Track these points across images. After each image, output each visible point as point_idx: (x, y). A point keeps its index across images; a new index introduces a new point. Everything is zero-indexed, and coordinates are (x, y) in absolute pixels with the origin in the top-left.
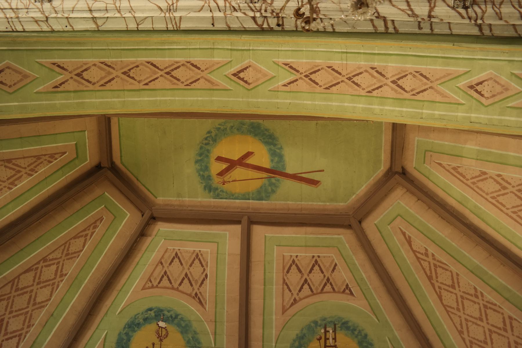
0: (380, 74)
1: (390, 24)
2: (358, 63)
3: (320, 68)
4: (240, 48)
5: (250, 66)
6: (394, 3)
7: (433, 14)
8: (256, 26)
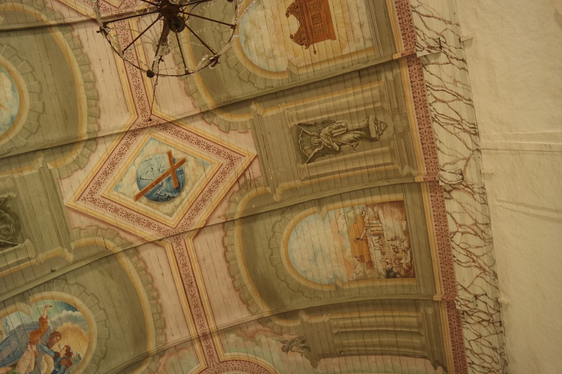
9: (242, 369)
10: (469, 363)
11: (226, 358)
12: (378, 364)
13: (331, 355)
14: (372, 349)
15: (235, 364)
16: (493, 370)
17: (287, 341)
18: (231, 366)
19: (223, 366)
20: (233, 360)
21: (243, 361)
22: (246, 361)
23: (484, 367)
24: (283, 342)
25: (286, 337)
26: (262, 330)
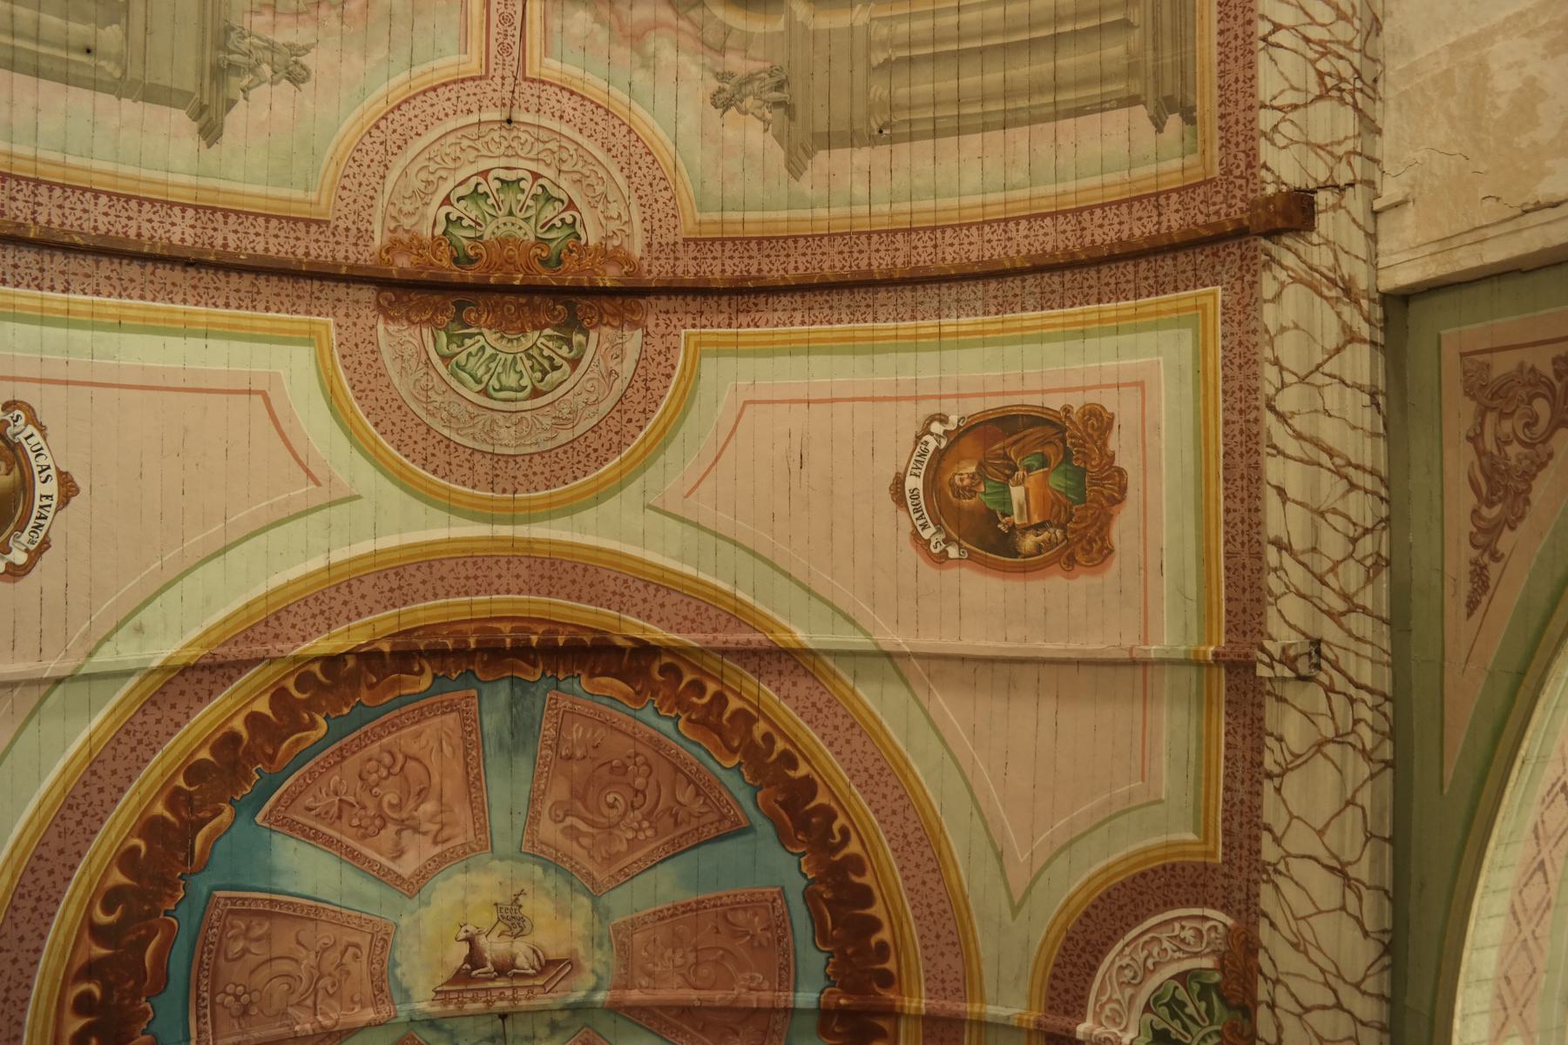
9: (579, 125)
10: (1264, 39)
11: (544, 71)
12: (987, 163)
13: (852, 139)
14: (977, 109)
15: (565, 101)
16: (1334, 47)
17: (732, 75)
18: (553, 102)
19: (528, 91)
20: (562, 89)
21: (592, 102)
22: (598, 106)
23: (1307, 40)
24: (722, 77)
25: (735, 63)
26: (670, 26)
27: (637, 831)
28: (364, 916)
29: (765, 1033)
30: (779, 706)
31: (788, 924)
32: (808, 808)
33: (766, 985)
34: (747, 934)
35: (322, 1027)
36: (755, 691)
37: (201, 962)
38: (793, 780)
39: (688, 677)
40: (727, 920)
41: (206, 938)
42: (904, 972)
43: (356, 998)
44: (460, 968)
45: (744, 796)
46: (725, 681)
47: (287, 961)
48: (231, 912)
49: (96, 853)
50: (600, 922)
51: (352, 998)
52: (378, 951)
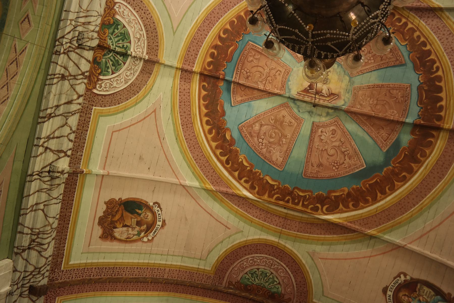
0: (4, 102)
1: (43, 120)
2: (14, 90)
3: (18, 68)
4: (41, 22)
5: (30, 26)
6: (60, 129)
7: (48, 150)
8: (58, 37)
27: (369, 60)
28: (285, 63)
29: (392, 130)
30: (425, 27)
31: (410, 96)
32: (426, 60)
33: (397, 115)
34: (395, 97)
35: (266, 89)
36: (418, 22)
37: (241, 59)
38: (424, 50)
39: (397, 17)
40: (390, 92)
41: (244, 53)
42: (447, 116)
43: (276, 86)
44: (306, 88)
45: (406, 54)
46: (409, 19)
47: (261, 68)
48: (252, 48)
49: (225, 17)
50: (350, 85)
51: (275, 86)
52: (286, 75)
